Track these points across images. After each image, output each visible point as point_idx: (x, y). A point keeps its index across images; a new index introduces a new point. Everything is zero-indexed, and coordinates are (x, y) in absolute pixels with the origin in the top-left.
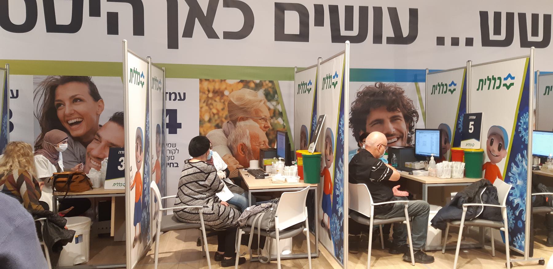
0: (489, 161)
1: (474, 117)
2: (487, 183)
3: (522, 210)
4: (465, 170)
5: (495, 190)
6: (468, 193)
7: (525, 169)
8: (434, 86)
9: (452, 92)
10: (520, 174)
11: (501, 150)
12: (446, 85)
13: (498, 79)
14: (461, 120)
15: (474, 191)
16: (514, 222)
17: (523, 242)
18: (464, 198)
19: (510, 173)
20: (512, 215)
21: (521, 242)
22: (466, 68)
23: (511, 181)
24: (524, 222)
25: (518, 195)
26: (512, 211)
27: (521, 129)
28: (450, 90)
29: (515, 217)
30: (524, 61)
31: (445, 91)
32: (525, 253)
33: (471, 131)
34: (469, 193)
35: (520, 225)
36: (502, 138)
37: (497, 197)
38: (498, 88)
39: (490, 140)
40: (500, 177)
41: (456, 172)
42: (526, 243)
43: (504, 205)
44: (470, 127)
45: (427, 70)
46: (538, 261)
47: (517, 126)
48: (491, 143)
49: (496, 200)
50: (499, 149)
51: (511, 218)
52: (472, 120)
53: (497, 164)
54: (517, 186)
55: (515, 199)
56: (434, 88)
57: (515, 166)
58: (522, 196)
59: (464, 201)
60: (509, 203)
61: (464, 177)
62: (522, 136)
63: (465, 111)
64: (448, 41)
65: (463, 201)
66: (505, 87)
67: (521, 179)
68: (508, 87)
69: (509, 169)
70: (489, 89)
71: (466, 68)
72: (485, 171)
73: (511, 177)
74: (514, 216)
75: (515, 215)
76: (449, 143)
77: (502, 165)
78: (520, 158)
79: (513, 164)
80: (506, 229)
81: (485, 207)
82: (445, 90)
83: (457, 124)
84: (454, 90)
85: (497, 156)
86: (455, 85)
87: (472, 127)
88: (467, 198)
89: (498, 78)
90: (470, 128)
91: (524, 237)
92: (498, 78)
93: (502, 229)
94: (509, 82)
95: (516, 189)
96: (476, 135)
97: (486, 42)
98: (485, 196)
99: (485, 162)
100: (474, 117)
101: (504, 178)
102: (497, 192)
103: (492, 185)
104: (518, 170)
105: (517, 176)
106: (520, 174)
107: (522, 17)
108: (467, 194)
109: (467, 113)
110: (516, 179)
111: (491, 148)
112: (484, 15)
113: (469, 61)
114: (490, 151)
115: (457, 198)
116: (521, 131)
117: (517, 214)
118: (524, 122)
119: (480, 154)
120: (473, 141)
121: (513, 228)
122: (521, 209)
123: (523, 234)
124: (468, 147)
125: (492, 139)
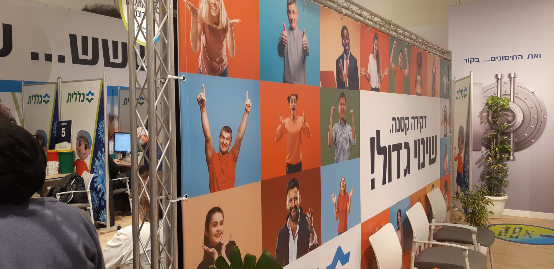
0: (79, 158)
1: (66, 124)
2: (76, 175)
3: (104, 192)
4: (59, 167)
5: (82, 180)
6: (61, 185)
7: (104, 162)
8: (30, 97)
9: (46, 103)
10: (100, 166)
11: (87, 149)
12: (41, 96)
13: (82, 95)
14: (55, 126)
15: (65, 183)
16: (99, 202)
17: (105, 216)
18: (57, 189)
19: (94, 166)
20: (97, 197)
21: (104, 216)
22: (57, 83)
24: (105, 201)
25: (100, 182)
27: (99, 132)
28: (44, 101)
29: (99, 199)
30: (99, 82)
31: (40, 101)
32: (106, 224)
33: (63, 136)
34: (61, 184)
35: (103, 204)
36: (87, 140)
37: (84, 185)
38: (83, 101)
39: (79, 142)
40: (87, 170)
41: (51, 170)
42: (108, 216)
43: (88, 190)
44: (63, 132)
45: (23, 82)
46: (117, 227)
47: (97, 131)
48: (79, 144)
49: (83, 187)
50: (86, 149)
51: (96, 200)
52: (64, 126)
53: (84, 160)
54: (99, 175)
55: (98, 185)
56: (30, 98)
58: (103, 182)
59: (57, 191)
60: (93, 188)
61: (58, 174)
62: (101, 138)
63: (58, 119)
64: (42, 57)
65: (57, 191)
66: (87, 101)
67: (101, 170)
68: (90, 101)
69: (93, 163)
70: (76, 102)
71: (57, 83)
72: (76, 166)
73: (95, 169)
74: (98, 198)
75: (99, 197)
76: (46, 146)
77: (88, 161)
78: (100, 154)
79: (96, 159)
80: (91, 208)
81: (74, 193)
82: (40, 100)
83: (52, 130)
84: (48, 101)
85: (84, 154)
86: (49, 97)
87: (64, 132)
88: (60, 188)
89: (82, 93)
90: (62, 133)
91: (106, 212)
92: (82, 93)
93: (88, 208)
94: (90, 97)
95: (98, 177)
96: (68, 139)
97: (76, 60)
98: (75, 185)
99: (76, 160)
100: (66, 124)
101: (90, 170)
102: (83, 181)
103: (80, 176)
104: (99, 163)
105: (99, 168)
106: (100, 166)
107: (105, 42)
108: (60, 185)
109: (60, 121)
110: (98, 170)
111: (80, 148)
112: (73, 38)
113: (59, 78)
114: (79, 151)
115: (52, 190)
116: (100, 134)
117: (100, 195)
118: (101, 128)
119: (72, 154)
120: (65, 143)
121: (98, 207)
122: (103, 191)
123: (105, 209)
124: (61, 149)
125: (80, 141)
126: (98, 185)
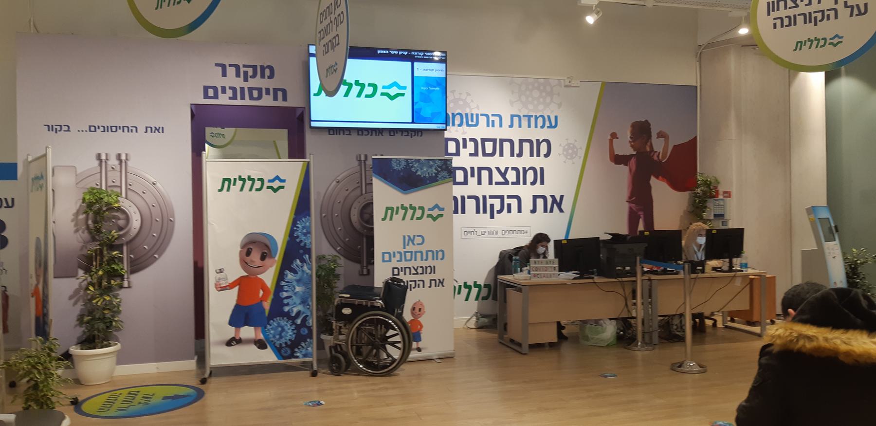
20: (291, 325)
23: (286, 290)
26: (290, 322)
55: (294, 308)
57: (292, 273)
73: (284, 285)
74: (294, 326)
105: (295, 283)
110: (294, 287)
126: (294, 308)
